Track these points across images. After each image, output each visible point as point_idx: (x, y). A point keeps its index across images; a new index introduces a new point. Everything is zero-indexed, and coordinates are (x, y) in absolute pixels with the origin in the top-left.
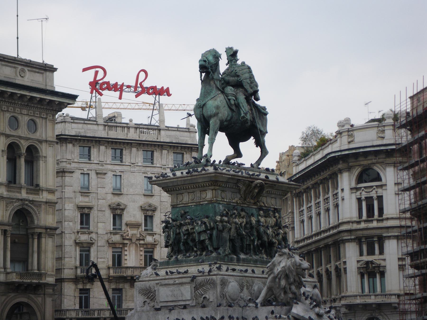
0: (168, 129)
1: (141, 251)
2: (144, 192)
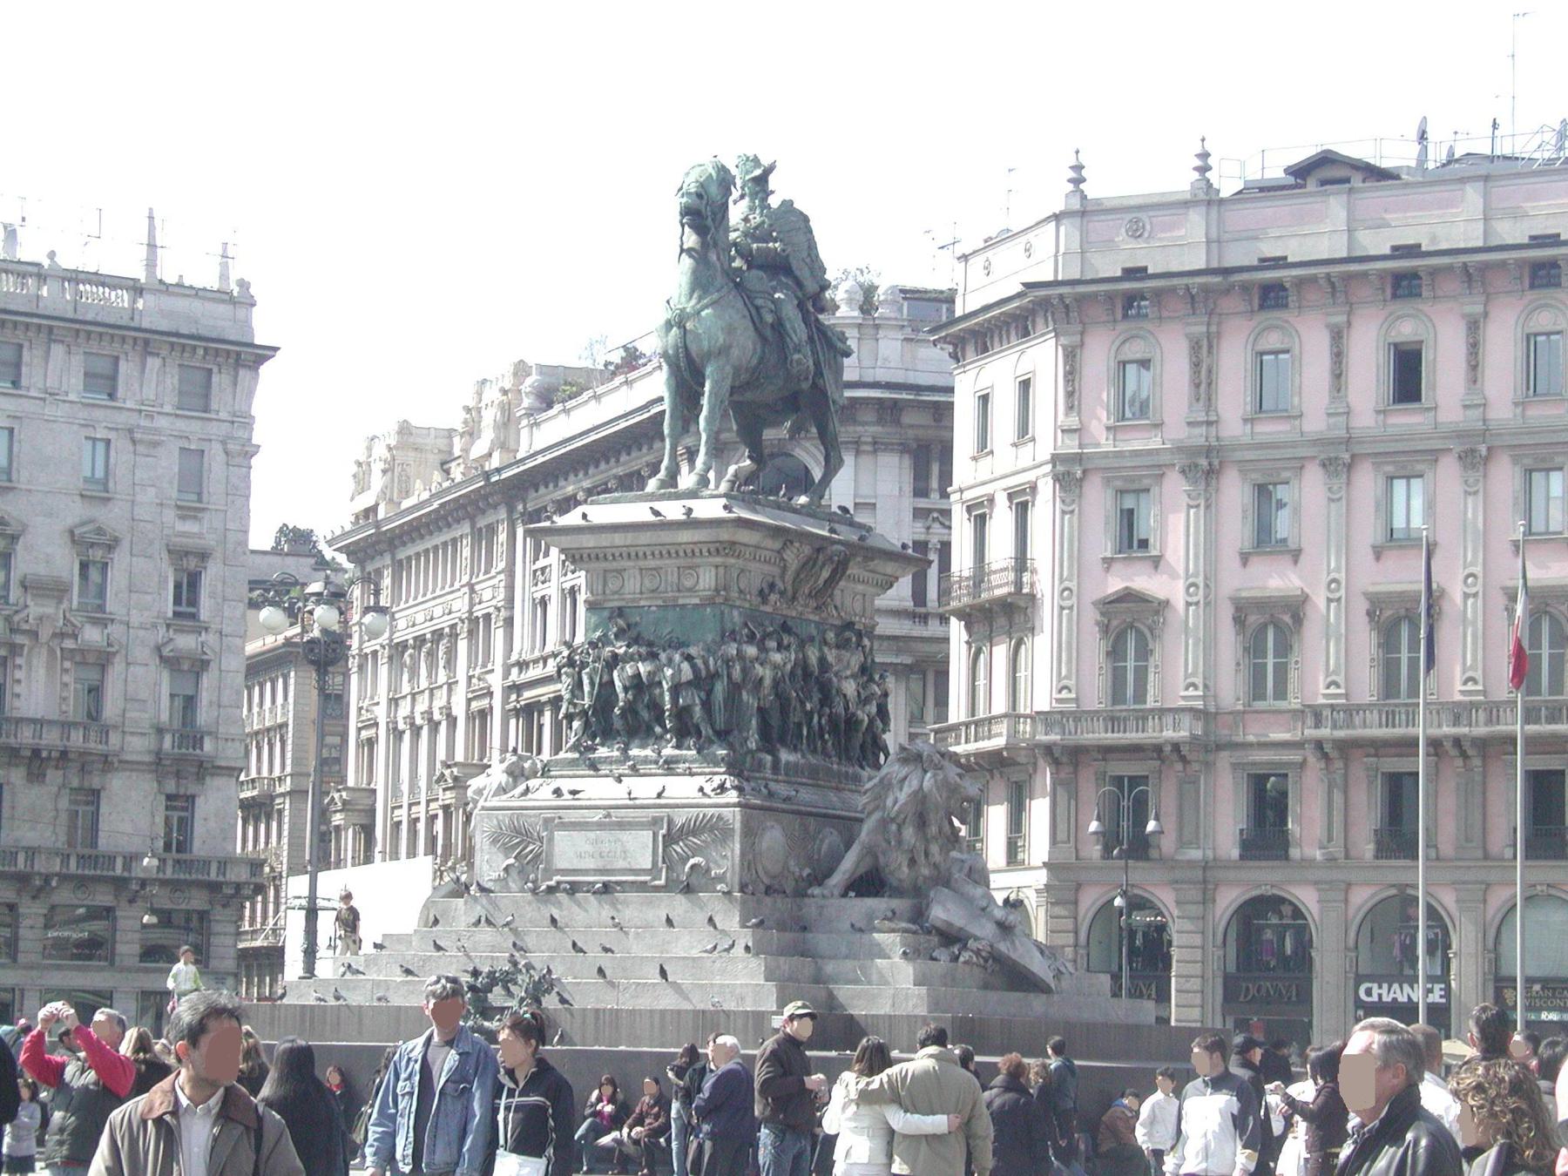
0: (164, 288)
1: (66, 671)
2: (81, 485)
